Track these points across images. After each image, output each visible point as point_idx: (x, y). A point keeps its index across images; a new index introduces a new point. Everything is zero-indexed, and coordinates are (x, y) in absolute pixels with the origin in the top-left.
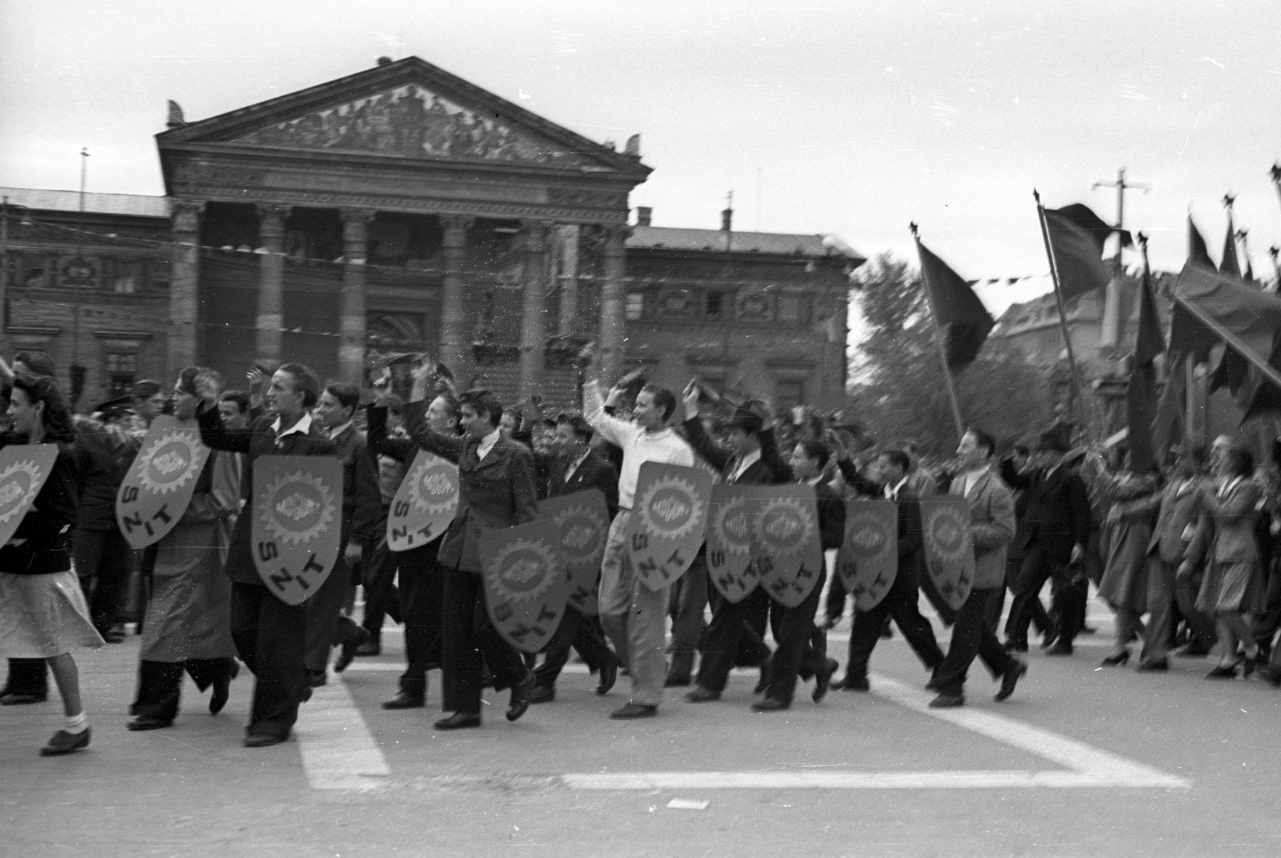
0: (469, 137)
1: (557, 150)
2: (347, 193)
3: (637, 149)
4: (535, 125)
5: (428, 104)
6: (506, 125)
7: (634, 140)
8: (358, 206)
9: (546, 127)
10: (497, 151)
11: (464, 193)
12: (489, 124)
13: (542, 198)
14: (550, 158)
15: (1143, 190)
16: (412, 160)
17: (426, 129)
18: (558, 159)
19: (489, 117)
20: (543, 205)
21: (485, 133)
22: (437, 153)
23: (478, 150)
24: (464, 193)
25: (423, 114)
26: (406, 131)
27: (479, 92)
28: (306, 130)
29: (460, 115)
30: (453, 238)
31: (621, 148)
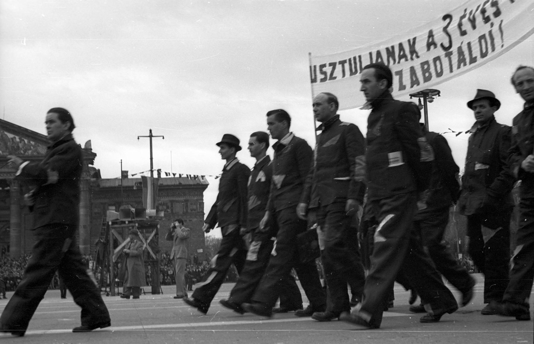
0: (18, 147)
3: (90, 145)
6: (33, 141)
7: (88, 143)
10: (30, 152)
12: (26, 141)
15: (162, 137)
19: (25, 139)
23: (22, 152)
31: (83, 147)
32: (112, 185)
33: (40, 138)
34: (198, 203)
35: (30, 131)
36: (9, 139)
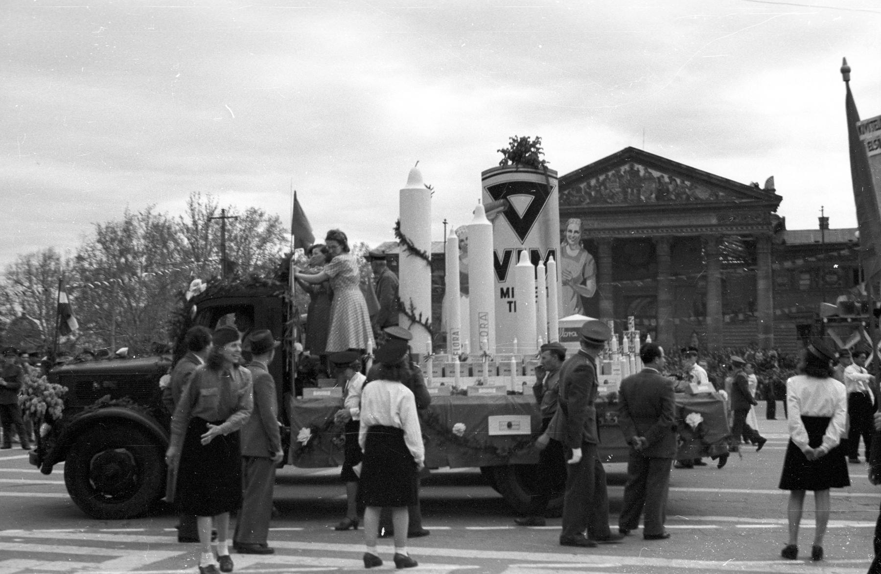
0: (668, 190)
1: (722, 192)
2: (596, 229)
3: (773, 184)
5: (642, 173)
6: (688, 181)
7: (770, 181)
8: (604, 236)
9: (712, 178)
11: (665, 223)
12: (678, 181)
13: (714, 221)
14: (717, 196)
16: (633, 207)
18: (722, 196)
19: (678, 177)
20: (714, 225)
23: (673, 197)
24: (665, 223)
26: (629, 190)
28: (573, 196)
30: (663, 250)
31: (762, 186)
32: (805, 241)
36: (654, 178)
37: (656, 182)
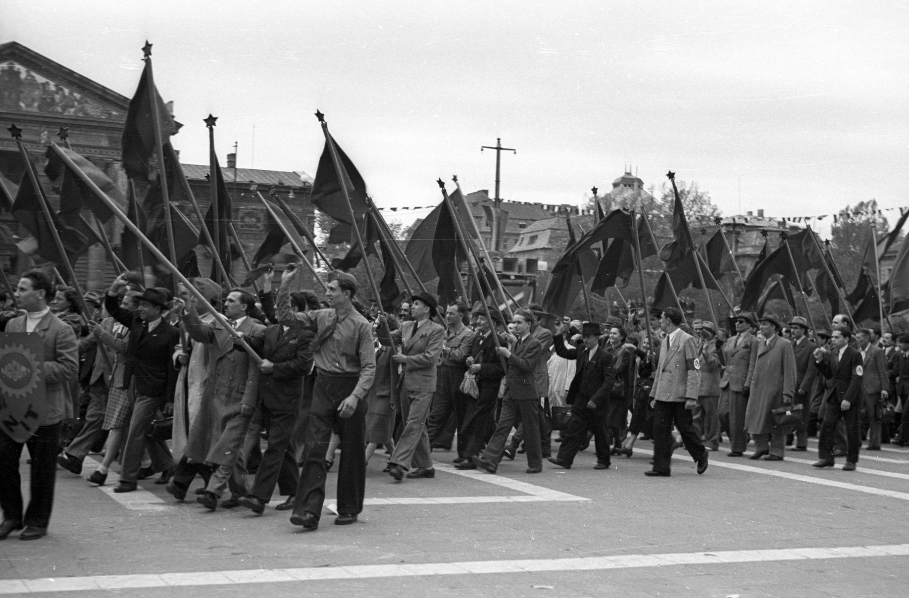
0: (53, 99)
1: (117, 111)
4: (100, 92)
5: (23, 75)
6: (79, 93)
9: (107, 93)
10: (72, 110)
12: (66, 91)
13: (105, 143)
14: (110, 114)
16: (12, 114)
17: (22, 92)
18: (115, 116)
19: (66, 87)
21: (64, 96)
22: (29, 109)
23: (59, 109)
25: (20, 82)
27: (60, 67)
29: (47, 84)
33: (93, 89)
34: (307, 218)
35: (77, 76)
36: (38, 84)
37: (39, 89)
